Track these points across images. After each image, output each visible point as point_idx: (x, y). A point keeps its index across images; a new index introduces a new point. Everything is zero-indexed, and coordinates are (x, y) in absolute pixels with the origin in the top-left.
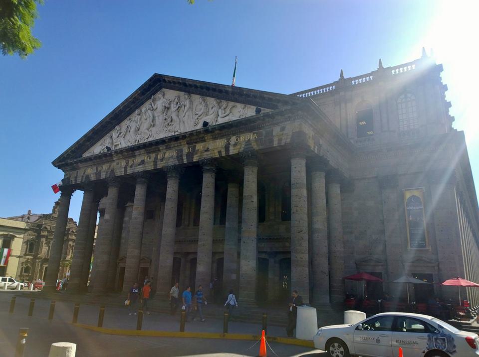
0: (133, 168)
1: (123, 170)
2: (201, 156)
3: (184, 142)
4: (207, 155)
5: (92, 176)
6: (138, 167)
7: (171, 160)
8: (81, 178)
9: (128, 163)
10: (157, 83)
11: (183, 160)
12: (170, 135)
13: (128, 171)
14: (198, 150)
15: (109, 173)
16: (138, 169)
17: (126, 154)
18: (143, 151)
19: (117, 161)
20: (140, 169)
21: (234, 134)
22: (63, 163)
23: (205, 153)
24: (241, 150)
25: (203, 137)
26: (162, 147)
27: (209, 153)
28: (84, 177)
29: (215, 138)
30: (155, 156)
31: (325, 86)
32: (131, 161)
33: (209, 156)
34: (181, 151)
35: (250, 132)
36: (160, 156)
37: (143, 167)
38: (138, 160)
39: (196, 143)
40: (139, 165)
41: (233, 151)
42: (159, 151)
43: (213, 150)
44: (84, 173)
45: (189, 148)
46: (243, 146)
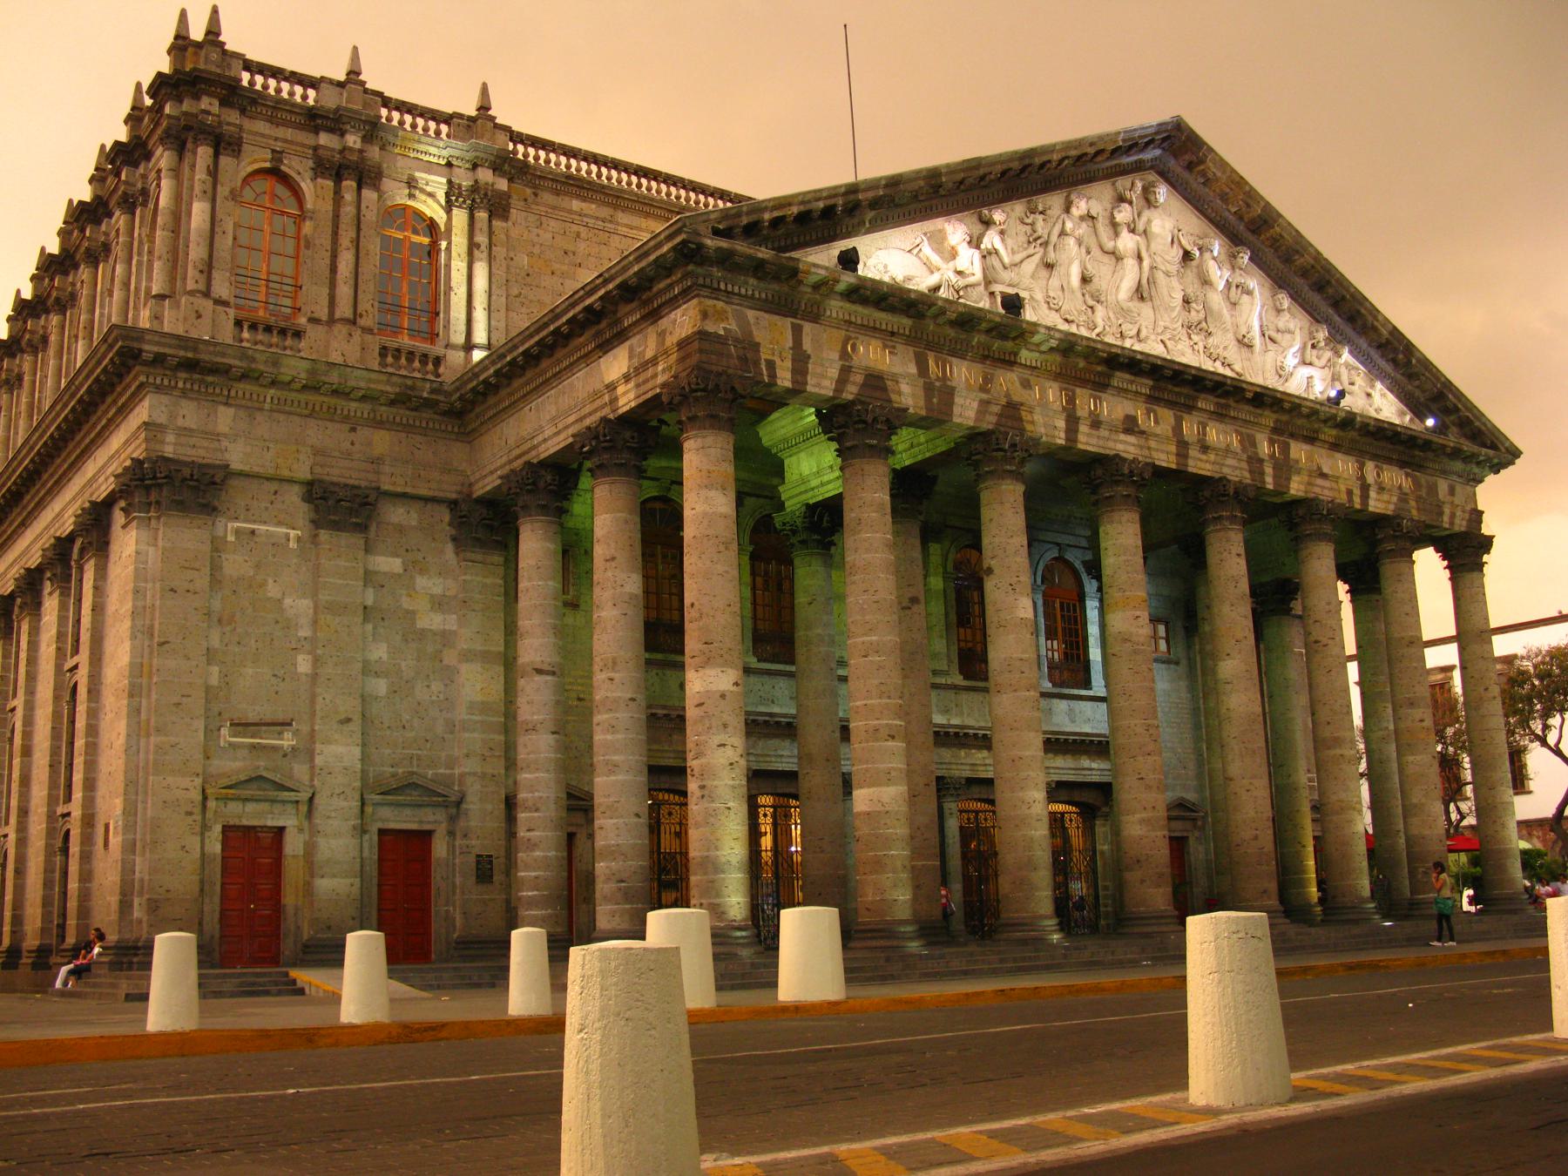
0: (1104, 433)
1: (1061, 424)
2: (1309, 484)
3: (1269, 418)
4: (1324, 491)
5: (905, 388)
6: (1122, 437)
7: (1230, 461)
8: (834, 372)
9: (1071, 400)
10: (1172, 156)
11: (1262, 473)
12: (1208, 366)
13: (1081, 438)
14: (1297, 461)
15: (996, 409)
16: (1120, 447)
17: (1082, 364)
18: (1145, 385)
19: (1026, 373)
20: (1126, 446)
21: (1374, 457)
22: (764, 253)
23: (1319, 481)
24: (1389, 509)
25: (1317, 432)
26: (1206, 403)
27: (1327, 484)
28: (859, 379)
29: (1335, 447)
30: (1172, 420)
31: (615, 165)
32: (1085, 402)
33: (1326, 492)
34: (1254, 444)
35: (1401, 467)
36: (1190, 428)
37: (1141, 447)
38: (1113, 408)
39: (1292, 436)
40: (1127, 431)
41: (1376, 505)
42: (1190, 408)
43: (1336, 479)
44: (844, 355)
45: (1271, 442)
46: (1395, 499)
